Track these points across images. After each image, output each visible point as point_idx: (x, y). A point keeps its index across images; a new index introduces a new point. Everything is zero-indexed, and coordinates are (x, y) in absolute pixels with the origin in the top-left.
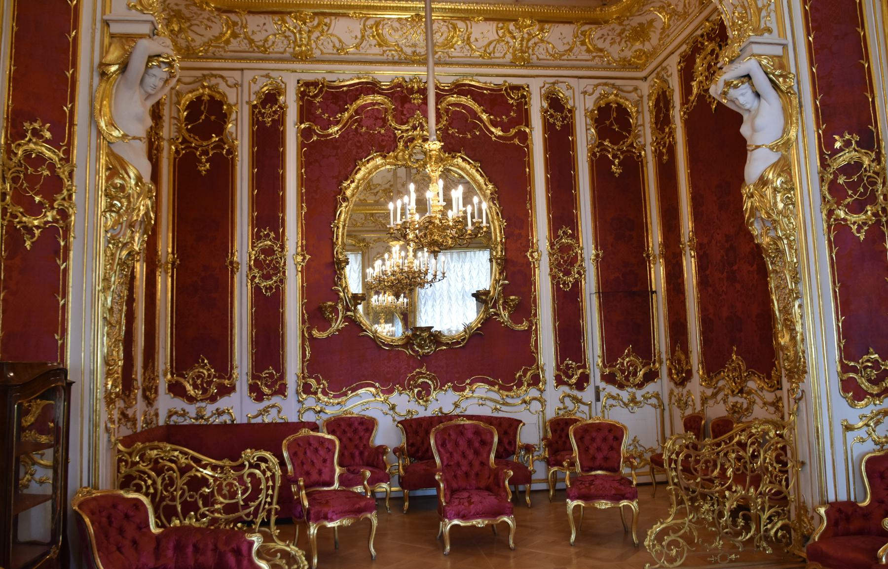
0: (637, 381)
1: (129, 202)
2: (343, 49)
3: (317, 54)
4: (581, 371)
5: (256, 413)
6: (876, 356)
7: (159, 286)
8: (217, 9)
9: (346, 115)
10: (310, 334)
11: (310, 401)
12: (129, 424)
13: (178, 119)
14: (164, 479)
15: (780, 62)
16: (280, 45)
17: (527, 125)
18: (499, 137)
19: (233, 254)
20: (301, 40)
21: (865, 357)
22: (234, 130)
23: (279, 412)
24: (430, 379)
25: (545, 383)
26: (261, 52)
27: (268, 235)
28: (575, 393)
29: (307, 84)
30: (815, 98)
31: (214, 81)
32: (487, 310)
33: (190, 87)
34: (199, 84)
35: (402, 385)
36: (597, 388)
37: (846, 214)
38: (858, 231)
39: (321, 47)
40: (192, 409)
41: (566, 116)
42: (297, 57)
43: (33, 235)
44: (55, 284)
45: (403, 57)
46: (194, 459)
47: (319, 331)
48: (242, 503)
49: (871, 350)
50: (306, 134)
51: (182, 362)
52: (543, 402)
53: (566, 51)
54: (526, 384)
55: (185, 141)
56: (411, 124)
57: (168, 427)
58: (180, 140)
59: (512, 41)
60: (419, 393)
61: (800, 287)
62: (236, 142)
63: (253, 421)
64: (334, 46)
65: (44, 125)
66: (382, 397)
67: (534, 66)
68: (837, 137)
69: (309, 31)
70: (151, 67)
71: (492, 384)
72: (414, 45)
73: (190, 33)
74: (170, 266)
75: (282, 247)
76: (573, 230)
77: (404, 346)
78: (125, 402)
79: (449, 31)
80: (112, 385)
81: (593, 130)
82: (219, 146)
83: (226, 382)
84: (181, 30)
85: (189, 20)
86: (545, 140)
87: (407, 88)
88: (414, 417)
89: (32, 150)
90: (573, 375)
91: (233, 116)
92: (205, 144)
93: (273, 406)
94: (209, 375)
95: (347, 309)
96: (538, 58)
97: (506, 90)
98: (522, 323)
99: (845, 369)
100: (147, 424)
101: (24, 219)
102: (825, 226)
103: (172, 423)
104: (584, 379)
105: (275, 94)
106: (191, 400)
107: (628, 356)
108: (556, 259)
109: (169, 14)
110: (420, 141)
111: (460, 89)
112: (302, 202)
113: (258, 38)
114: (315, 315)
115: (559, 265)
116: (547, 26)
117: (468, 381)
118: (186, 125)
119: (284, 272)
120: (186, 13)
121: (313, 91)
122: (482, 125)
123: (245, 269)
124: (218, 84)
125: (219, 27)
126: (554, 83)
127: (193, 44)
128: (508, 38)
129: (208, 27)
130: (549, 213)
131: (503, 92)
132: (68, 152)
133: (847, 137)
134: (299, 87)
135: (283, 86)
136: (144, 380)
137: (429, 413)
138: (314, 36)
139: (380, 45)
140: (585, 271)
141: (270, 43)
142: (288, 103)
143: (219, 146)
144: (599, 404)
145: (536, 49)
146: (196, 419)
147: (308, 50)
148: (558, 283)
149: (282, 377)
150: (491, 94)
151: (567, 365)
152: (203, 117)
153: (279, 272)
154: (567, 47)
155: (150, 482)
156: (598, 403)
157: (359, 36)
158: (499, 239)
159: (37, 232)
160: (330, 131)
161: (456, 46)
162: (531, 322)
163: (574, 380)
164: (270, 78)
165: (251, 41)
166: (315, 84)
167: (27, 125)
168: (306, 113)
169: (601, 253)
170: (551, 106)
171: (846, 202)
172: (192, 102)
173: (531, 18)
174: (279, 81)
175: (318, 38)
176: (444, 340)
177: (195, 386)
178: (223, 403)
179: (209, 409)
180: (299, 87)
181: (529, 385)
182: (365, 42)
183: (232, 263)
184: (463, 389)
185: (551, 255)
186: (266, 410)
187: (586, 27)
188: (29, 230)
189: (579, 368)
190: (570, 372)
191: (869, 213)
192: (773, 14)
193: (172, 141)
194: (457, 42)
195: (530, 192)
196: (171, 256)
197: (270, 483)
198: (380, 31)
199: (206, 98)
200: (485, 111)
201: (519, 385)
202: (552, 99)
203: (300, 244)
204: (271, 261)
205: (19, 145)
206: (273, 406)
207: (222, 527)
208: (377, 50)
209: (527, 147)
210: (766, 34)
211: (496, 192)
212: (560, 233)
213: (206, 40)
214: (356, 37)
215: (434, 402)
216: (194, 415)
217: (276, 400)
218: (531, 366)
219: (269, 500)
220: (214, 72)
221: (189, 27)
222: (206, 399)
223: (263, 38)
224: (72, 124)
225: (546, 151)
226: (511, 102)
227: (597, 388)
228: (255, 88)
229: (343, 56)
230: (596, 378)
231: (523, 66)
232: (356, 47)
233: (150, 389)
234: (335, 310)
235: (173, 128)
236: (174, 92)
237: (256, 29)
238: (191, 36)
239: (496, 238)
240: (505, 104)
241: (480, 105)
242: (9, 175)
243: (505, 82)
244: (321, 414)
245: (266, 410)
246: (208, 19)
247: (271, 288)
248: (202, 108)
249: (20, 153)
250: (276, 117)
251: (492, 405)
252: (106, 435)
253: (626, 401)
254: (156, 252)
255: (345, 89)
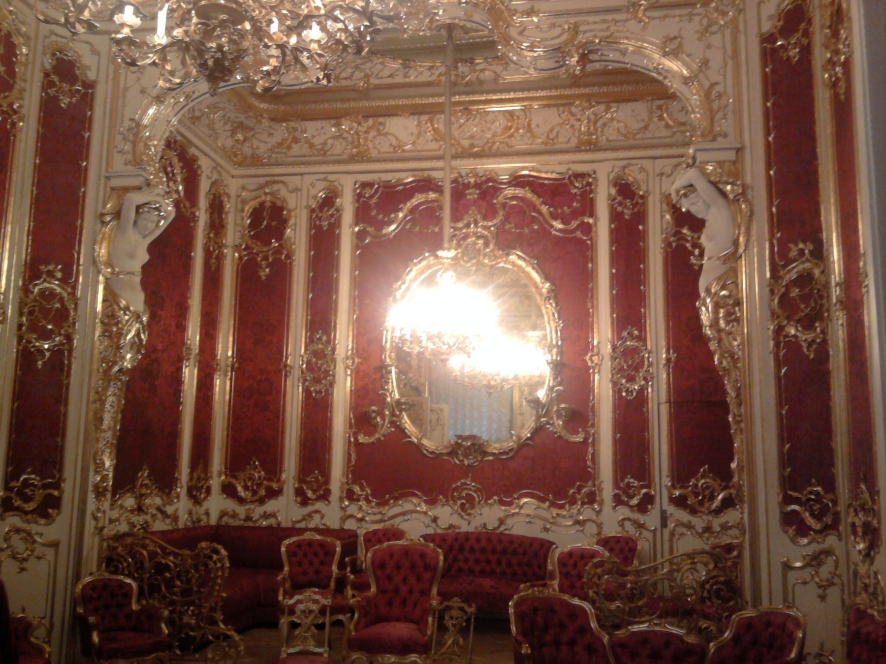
0: (714, 506)
1: (119, 329)
2: (400, 146)
3: (374, 153)
4: (644, 491)
5: (300, 518)
6: (819, 489)
7: (217, 389)
8: (272, 120)
9: (401, 215)
10: (356, 439)
11: (353, 509)
12: (168, 521)
13: (243, 226)
14: (136, 563)
15: (734, 170)
16: (339, 147)
17: (592, 214)
18: (560, 230)
19: (287, 358)
20: (359, 141)
21: (809, 489)
22: (293, 236)
23: (322, 518)
24: (475, 492)
25: (601, 503)
26: (322, 155)
27: (320, 339)
28: (637, 516)
29: (365, 185)
30: (770, 203)
31: (275, 187)
32: (538, 417)
33: (254, 194)
34: (261, 191)
35: (446, 497)
36: (663, 513)
37: (797, 330)
38: (808, 350)
39: (378, 146)
40: (241, 511)
41: (637, 203)
42: (353, 159)
43: (44, 356)
44: (60, 397)
45: (460, 150)
46: (161, 547)
47: (365, 435)
48: (195, 589)
49: (813, 480)
50: (360, 236)
51: (236, 463)
52: (600, 526)
53: (640, 129)
54: (580, 503)
55: (247, 248)
56: (465, 222)
57: (218, 526)
58: (243, 246)
59: (577, 124)
60: (463, 505)
61: (742, 410)
62: (293, 247)
63: (298, 526)
64: (391, 145)
65: (56, 267)
66: (424, 507)
67: (600, 150)
68: (792, 246)
69: (366, 132)
70: (142, 213)
71: (542, 500)
72: (472, 137)
73: (254, 141)
74: (229, 369)
75: (333, 350)
76: (640, 331)
77: (449, 454)
78: (162, 499)
79: (508, 120)
80: (100, 481)
81: (668, 217)
82: (278, 251)
83: (275, 486)
84: (245, 140)
85: (252, 129)
86: (612, 231)
87: (463, 184)
88: (457, 531)
89: (46, 288)
90: (635, 495)
91: (292, 222)
92: (265, 249)
93: (317, 512)
94: (259, 478)
95: (393, 414)
96: (608, 140)
97: (569, 178)
98: (577, 433)
99: (787, 500)
100: (193, 522)
101: (37, 344)
102: (772, 343)
103: (223, 523)
104: (648, 500)
105: (331, 198)
106: (241, 501)
107: (703, 477)
108: (619, 363)
109: (232, 126)
110: (474, 239)
111: (517, 181)
112: (354, 305)
113: (317, 141)
114: (362, 420)
115: (621, 370)
116: (614, 105)
117: (515, 496)
118: (249, 232)
119: (334, 376)
120: (247, 122)
121: (368, 192)
122: (541, 219)
123: (297, 373)
124: (278, 190)
125: (281, 132)
126: (624, 168)
127: (257, 152)
128: (573, 121)
129: (271, 135)
130: (612, 312)
131: (566, 181)
132: (74, 288)
133: (801, 246)
134: (357, 189)
135: (340, 188)
136: (191, 479)
137: (471, 529)
138: (370, 136)
139: (436, 140)
140: (652, 378)
141: (329, 145)
142: (344, 205)
143: (278, 251)
144: (666, 532)
145: (606, 129)
146: (245, 520)
147: (365, 151)
148: (620, 391)
149: (327, 481)
150: (553, 184)
151: (628, 483)
152: (265, 223)
153: (329, 375)
154: (642, 125)
155: (125, 564)
156: (664, 530)
157: (416, 132)
158: (554, 342)
159: (47, 354)
160: (384, 231)
161: (516, 134)
162: (587, 433)
163: (635, 501)
164: (328, 181)
165: (311, 146)
166: (370, 185)
167: (43, 268)
168: (362, 214)
169: (673, 356)
170: (620, 192)
171: (797, 317)
172: (255, 209)
173: (589, 101)
174: (336, 184)
175: (374, 137)
176: (490, 450)
177: (246, 488)
178: (271, 506)
179: (259, 510)
180: (357, 189)
181: (583, 503)
182: (421, 138)
183: (286, 366)
184: (510, 504)
185: (613, 358)
186: (310, 515)
187: (662, 102)
188: (41, 351)
189: (642, 487)
190: (631, 491)
191: (818, 330)
192: (730, 117)
193: (237, 248)
194: (517, 130)
195: (592, 289)
196: (231, 359)
197: (220, 573)
198: (436, 126)
199: (268, 204)
200: (545, 203)
201: (573, 502)
202: (621, 185)
203: (350, 347)
204: (322, 365)
205: (36, 285)
206: (317, 512)
207: (178, 608)
208: (434, 145)
209: (591, 239)
210: (720, 139)
211: (553, 291)
212: (625, 334)
213: (269, 146)
214: (412, 134)
215: (478, 517)
216: (242, 516)
217: (319, 505)
218: (586, 481)
219: (217, 588)
220: (276, 178)
221: (254, 135)
222: (256, 501)
223: (322, 141)
224: (78, 265)
225: (612, 243)
226: (574, 191)
227: (663, 513)
228: (313, 192)
229: (399, 154)
230: (662, 501)
231: (590, 150)
232: (413, 143)
233: (199, 489)
234: (381, 414)
235: (238, 235)
236: (239, 199)
237: (315, 133)
238: (256, 143)
239: (552, 340)
240: (566, 195)
241: (539, 196)
242: (26, 310)
243: (569, 169)
244: (363, 523)
245: (310, 515)
246: (270, 127)
247: (320, 392)
248: (265, 214)
249: (36, 290)
250: (332, 220)
251: (540, 523)
252: (93, 523)
253: (700, 531)
254: (213, 355)
255: (401, 187)
